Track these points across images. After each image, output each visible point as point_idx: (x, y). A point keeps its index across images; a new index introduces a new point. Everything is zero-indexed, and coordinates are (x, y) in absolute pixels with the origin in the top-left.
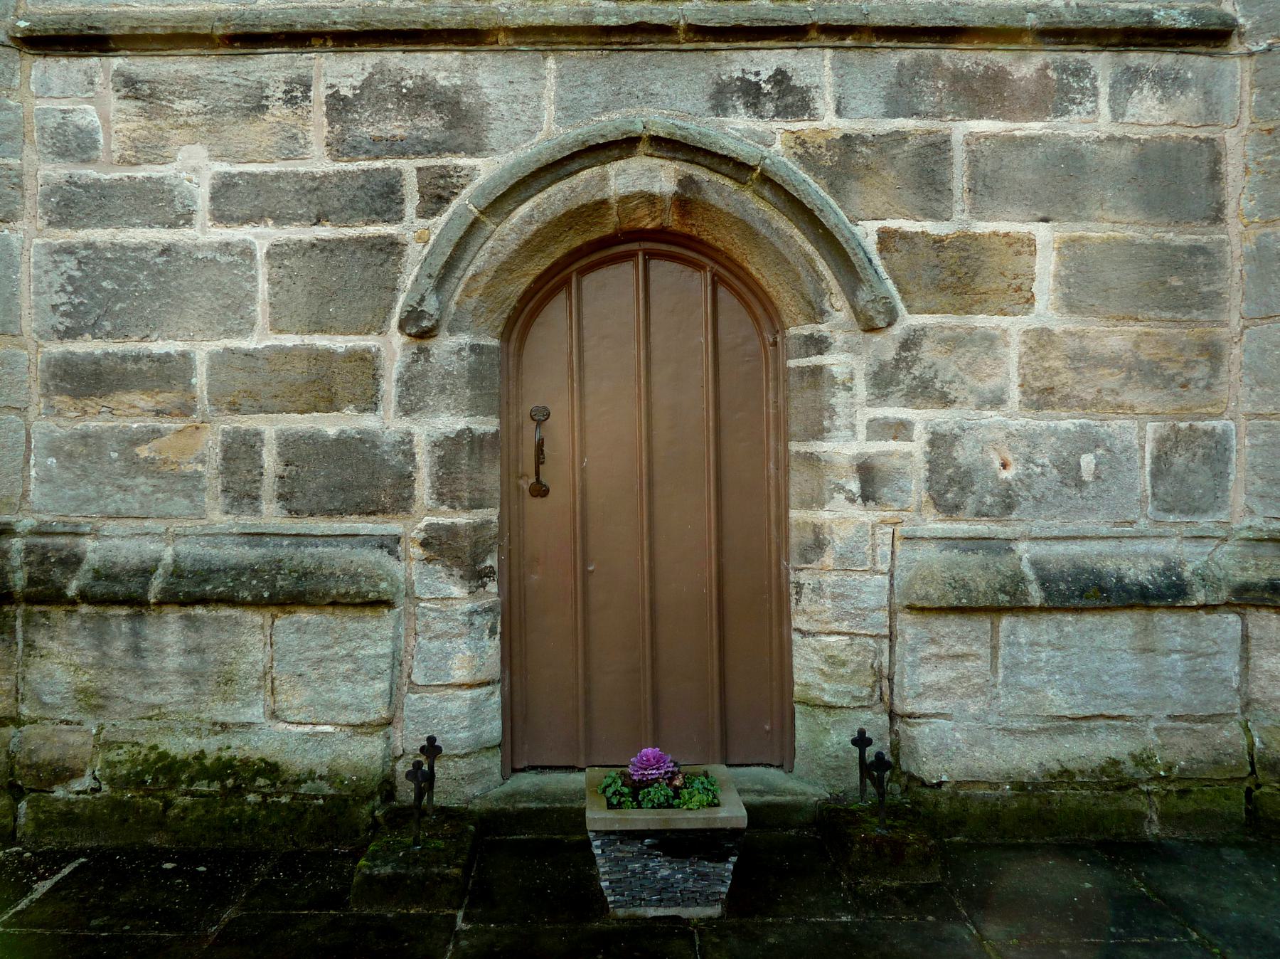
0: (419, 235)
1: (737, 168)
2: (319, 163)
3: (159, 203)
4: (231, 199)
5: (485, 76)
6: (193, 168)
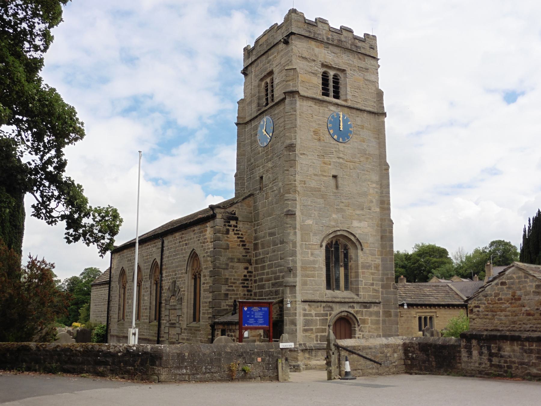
1: (351, 313)
2: (322, 312)
3: (311, 315)
4: (317, 315)
5: (334, 305)
6: (313, 312)
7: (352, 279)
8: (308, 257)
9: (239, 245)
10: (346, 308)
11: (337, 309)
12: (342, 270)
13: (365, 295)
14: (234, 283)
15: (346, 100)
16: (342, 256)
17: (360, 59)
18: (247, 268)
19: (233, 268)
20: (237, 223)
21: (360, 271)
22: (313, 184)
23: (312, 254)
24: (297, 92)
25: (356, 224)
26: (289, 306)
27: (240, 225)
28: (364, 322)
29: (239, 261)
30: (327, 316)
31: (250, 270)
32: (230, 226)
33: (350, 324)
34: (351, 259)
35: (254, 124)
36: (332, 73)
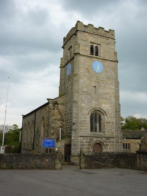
0: (91, 143)
1: (101, 142)
2: (88, 141)
3: (83, 142)
5: (94, 138)
6: (85, 141)
7: (102, 128)
8: (82, 118)
9: (59, 114)
10: (99, 139)
11: (95, 139)
12: (98, 124)
13: (107, 134)
14: (56, 129)
15: (100, 56)
16: (98, 119)
17: (107, 40)
18: (62, 123)
19: (56, 123)
20: (58, 106)
21: (106, 124)
22: (85, 90)
23: (84, 118)
24: (79, 54)
25: (103, 105)
26: (73, 138)
27: (59, 106)
28: (107, 145)
29: (59, 120)
30: (90, 142)
31: (63, 124)
32: (55, 107)
33: (101, 146)
34: (102, 119)
35: (66, 67)
36: (95, 45)
